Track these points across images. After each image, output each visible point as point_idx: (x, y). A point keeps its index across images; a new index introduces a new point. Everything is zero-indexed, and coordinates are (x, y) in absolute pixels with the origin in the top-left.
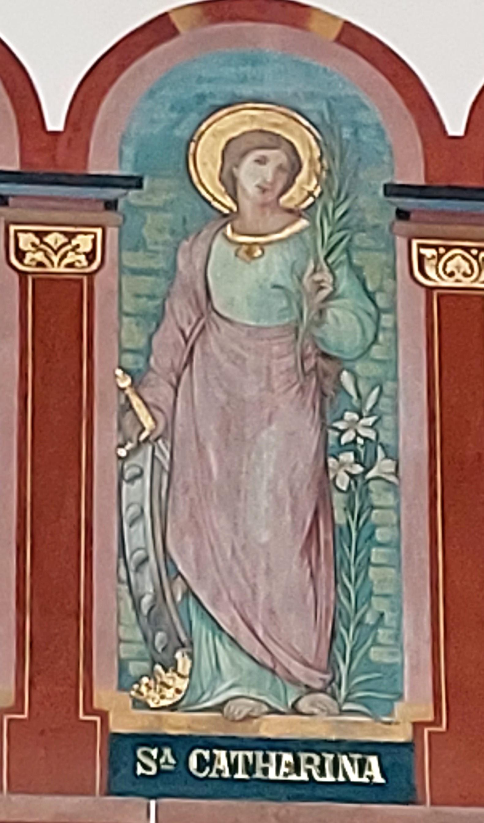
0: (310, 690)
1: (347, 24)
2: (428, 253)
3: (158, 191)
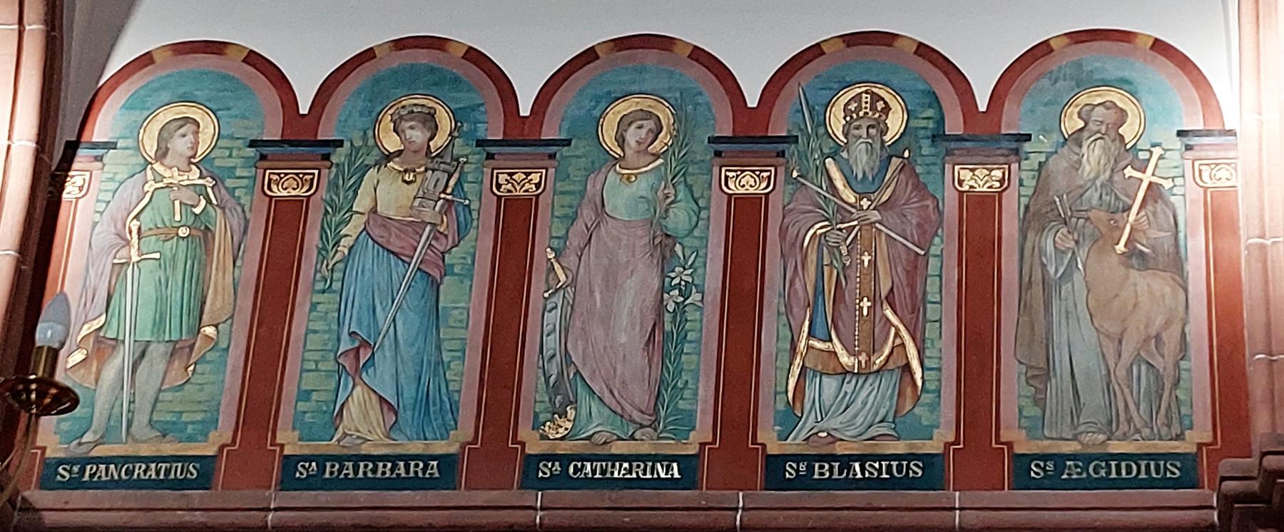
0: (642, 426)
1: (696, 47)
2: (731, 174)
3: (579, 147)
